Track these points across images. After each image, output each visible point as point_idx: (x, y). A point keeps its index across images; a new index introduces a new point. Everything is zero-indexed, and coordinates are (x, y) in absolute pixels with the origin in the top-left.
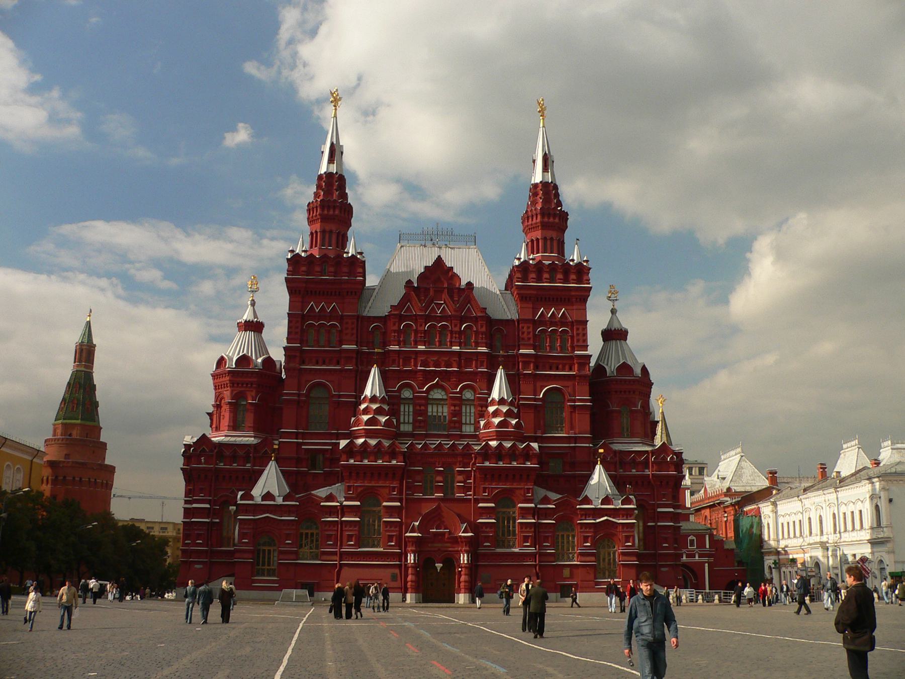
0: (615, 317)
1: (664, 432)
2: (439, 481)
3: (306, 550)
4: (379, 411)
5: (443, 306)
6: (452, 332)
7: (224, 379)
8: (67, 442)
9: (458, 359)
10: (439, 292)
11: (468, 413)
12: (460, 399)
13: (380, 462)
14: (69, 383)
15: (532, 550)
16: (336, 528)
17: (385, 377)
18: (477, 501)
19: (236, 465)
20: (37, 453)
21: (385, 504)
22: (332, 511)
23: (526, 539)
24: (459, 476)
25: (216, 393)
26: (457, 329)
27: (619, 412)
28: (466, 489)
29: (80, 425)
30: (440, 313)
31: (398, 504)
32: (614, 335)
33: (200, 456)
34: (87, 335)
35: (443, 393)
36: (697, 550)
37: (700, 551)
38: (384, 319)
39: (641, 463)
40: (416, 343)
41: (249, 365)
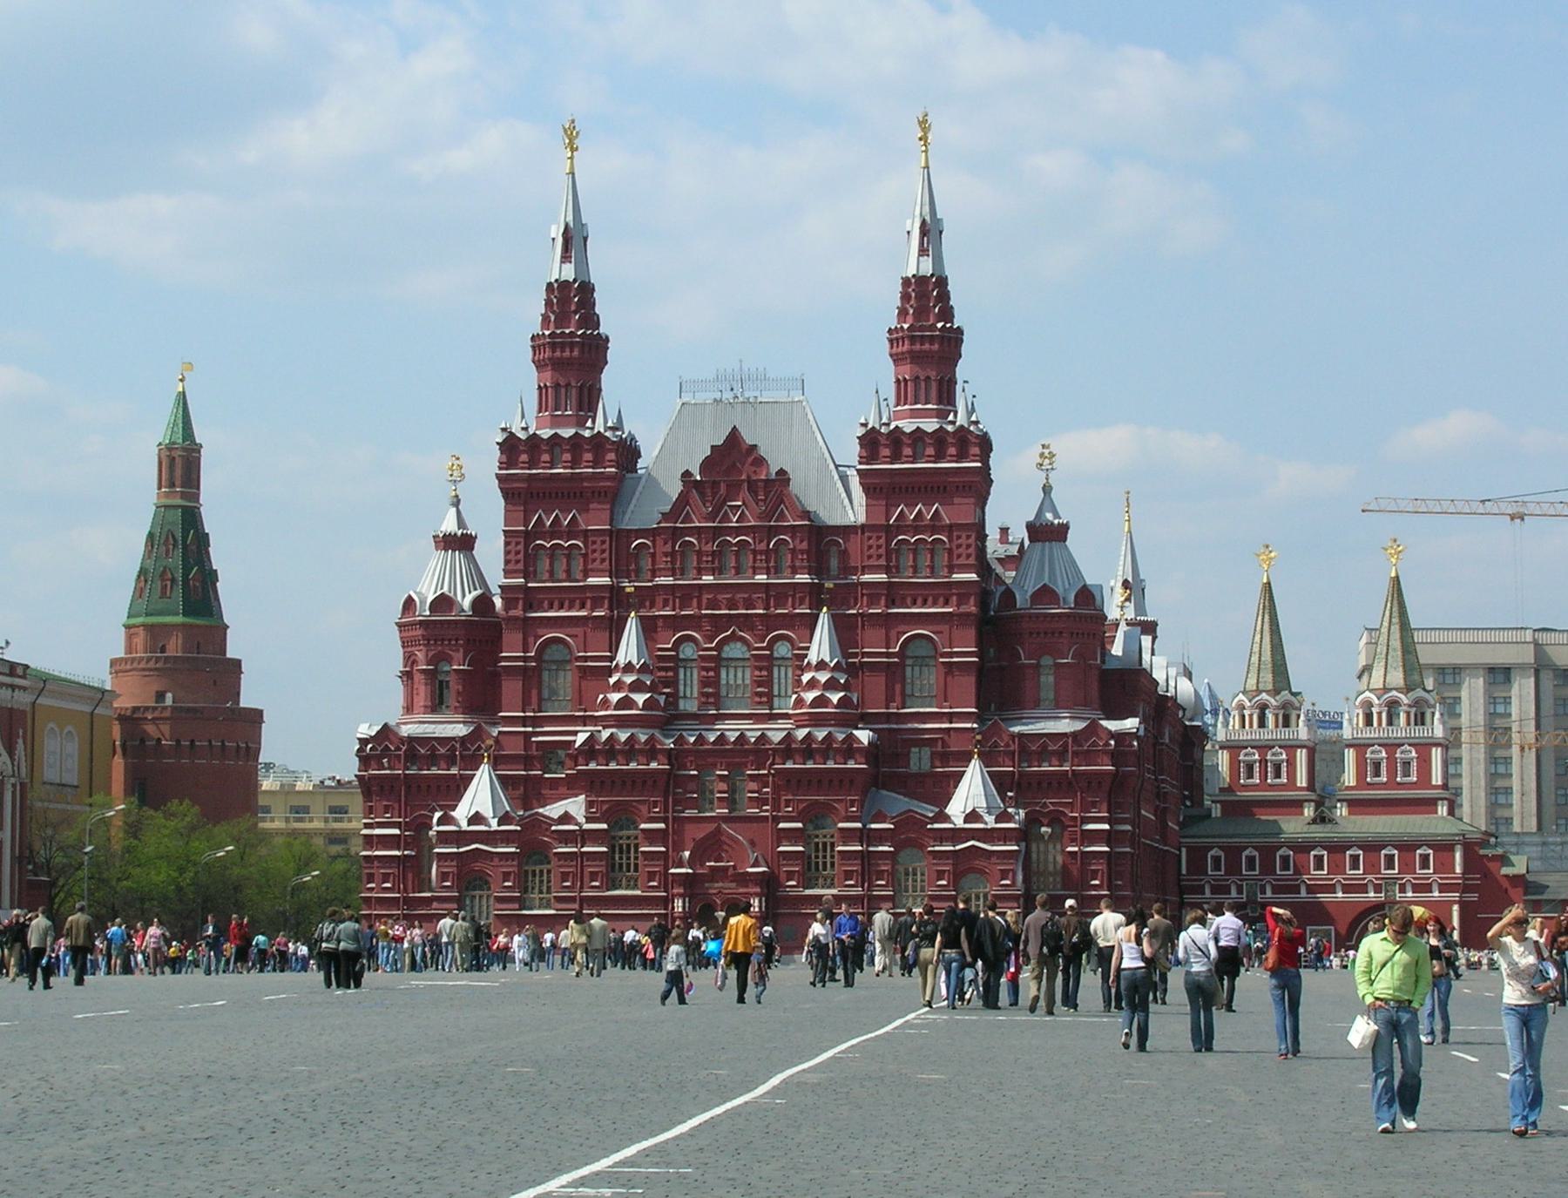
0: (1047, 502)
1: (1396, 620)
2: (719, 790)
3: (536, 896)
4: (637, 687)
5: (742, 512)
6: (755, 552)
7: (414, 633)
8: (157, 666)
9: (764, 596)
10: (733, 489)
12: (770, 658)
13: (633, 765)
14: (151, 536)
15: (858, 891)
16: (574, 863)
17: (649, 629)
18: (777, 820)
20: (101, 695)
21: (643, 826)
22: (566, 838)
23: (848, 875)
24: (751, 783)
25: (405, 653)
26: (762, 546)
28: (760, 802)
29: (184, 625)
30: (737, 522)
31: (662, 826)
32: (1048, 533)
33: (379, 758)
34: (181, 425)
35: (745, 648)
36: (1435, 877)
38: (651, 533)
39: (1054, 753)
40: (700, 572)
41: (451, 611)
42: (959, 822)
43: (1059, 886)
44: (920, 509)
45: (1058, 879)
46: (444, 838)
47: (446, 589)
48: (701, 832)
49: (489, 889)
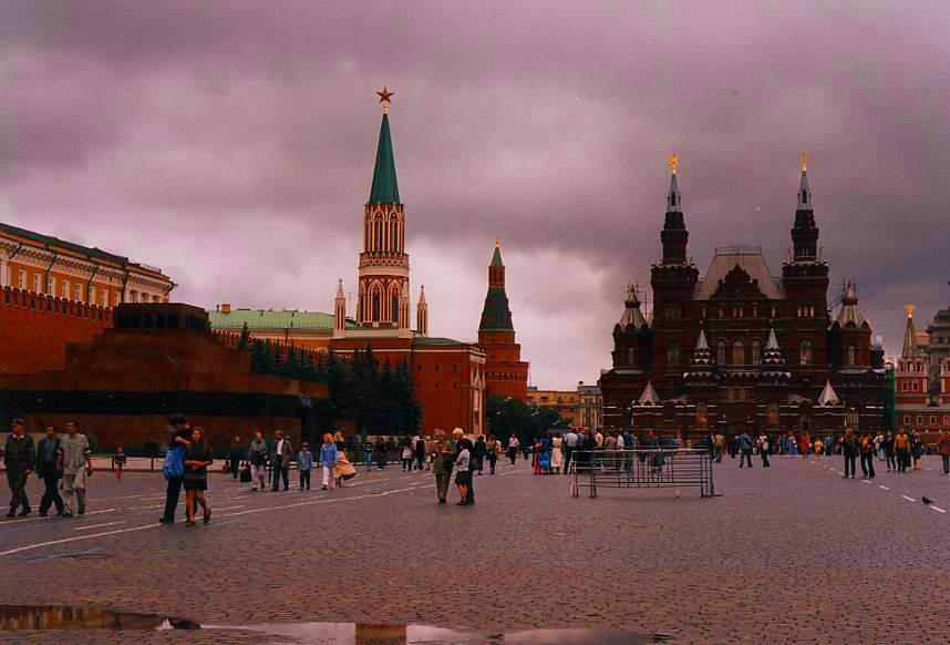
17: (708, 338)
42: (823, 405)
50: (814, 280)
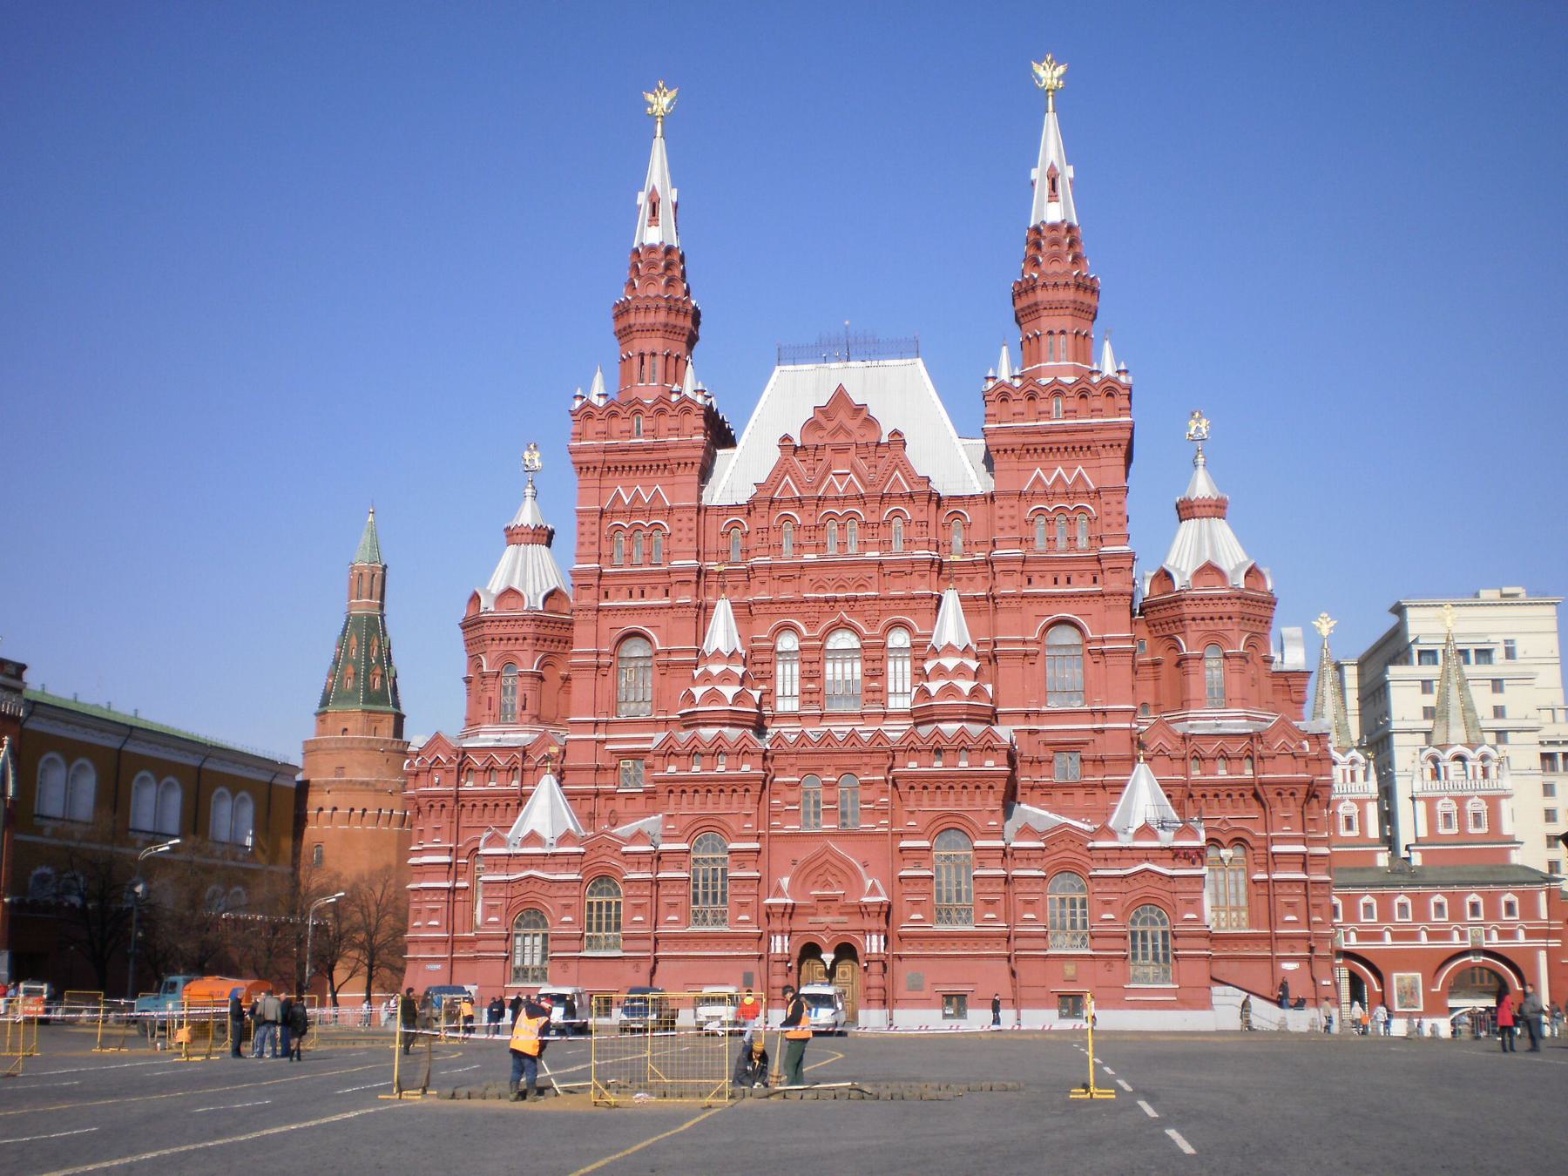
11: (899, 674)
15: (1000, 927)
17: (745, 613)
19: (494, 784)
22: (637, 860)
26: (874, 519)
27: (1201, 658)
30: (844, 492)
37: (1528, 925)
42: (1125, 841)
43: (1244, 924)
44: (1059, 475)
45: (1244, 914)
46: (495, 862)
47: (516, 586)
48: (805, 853)
49: (545, 925)
50: (1090, 429)
